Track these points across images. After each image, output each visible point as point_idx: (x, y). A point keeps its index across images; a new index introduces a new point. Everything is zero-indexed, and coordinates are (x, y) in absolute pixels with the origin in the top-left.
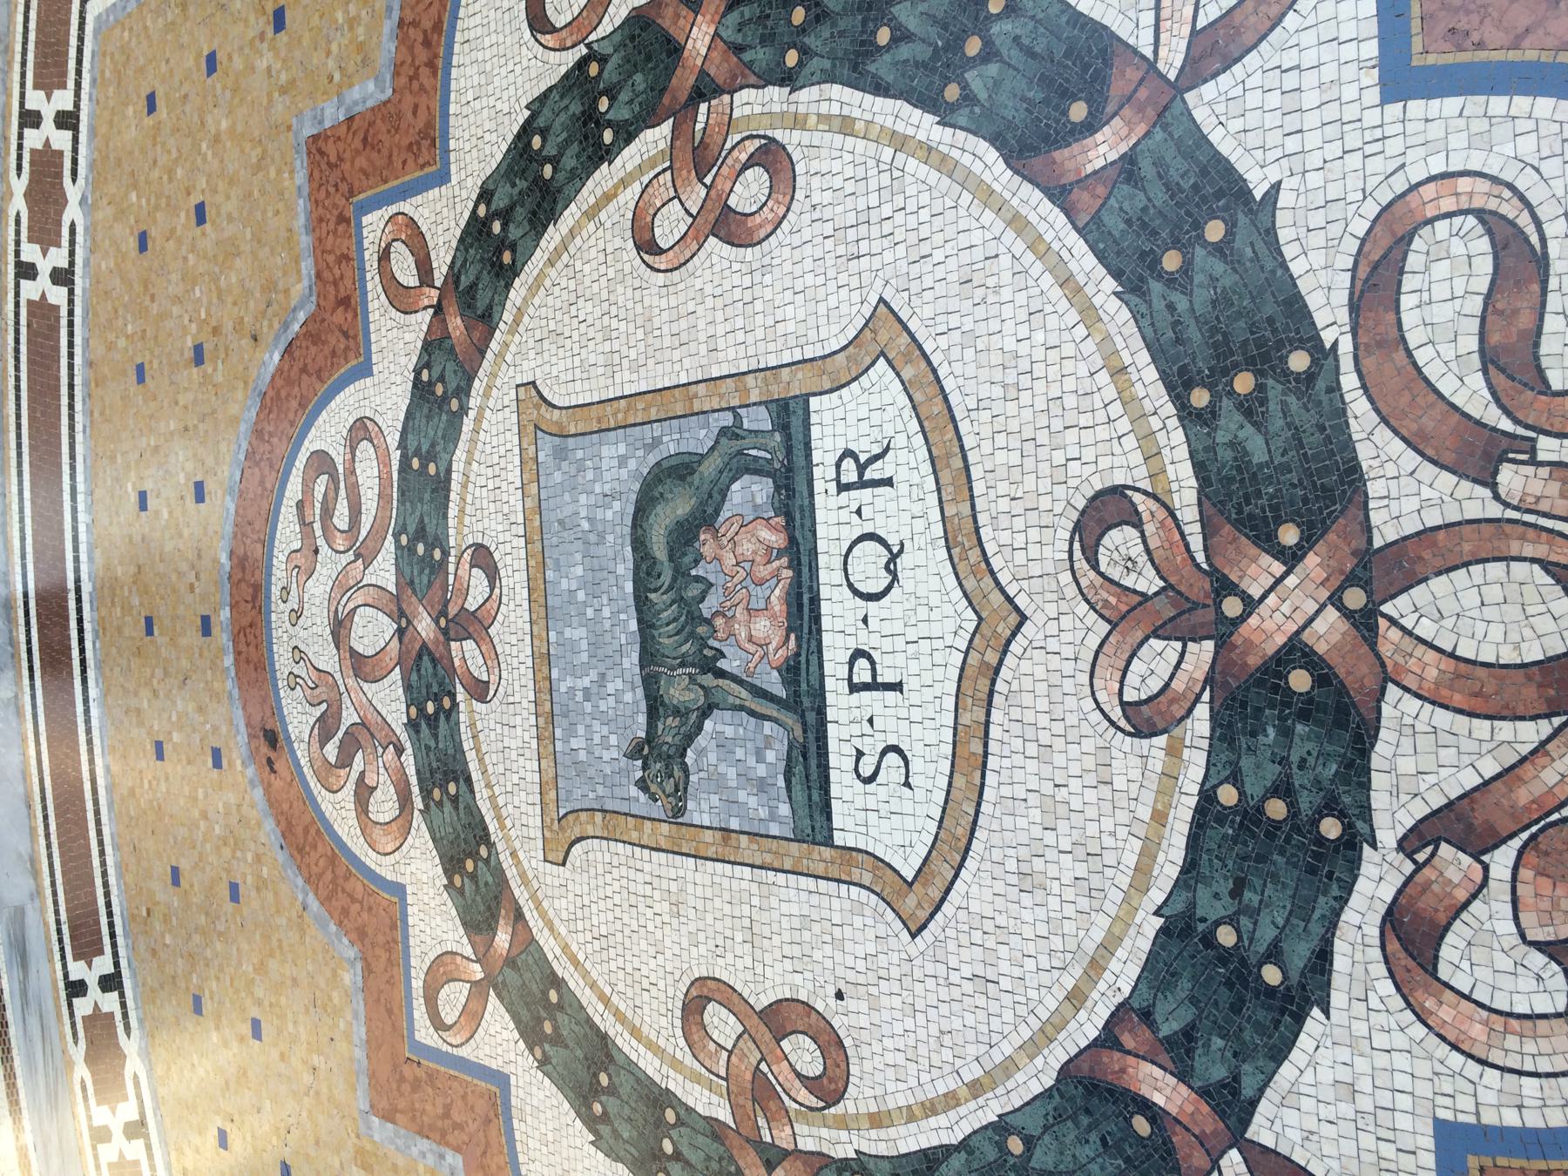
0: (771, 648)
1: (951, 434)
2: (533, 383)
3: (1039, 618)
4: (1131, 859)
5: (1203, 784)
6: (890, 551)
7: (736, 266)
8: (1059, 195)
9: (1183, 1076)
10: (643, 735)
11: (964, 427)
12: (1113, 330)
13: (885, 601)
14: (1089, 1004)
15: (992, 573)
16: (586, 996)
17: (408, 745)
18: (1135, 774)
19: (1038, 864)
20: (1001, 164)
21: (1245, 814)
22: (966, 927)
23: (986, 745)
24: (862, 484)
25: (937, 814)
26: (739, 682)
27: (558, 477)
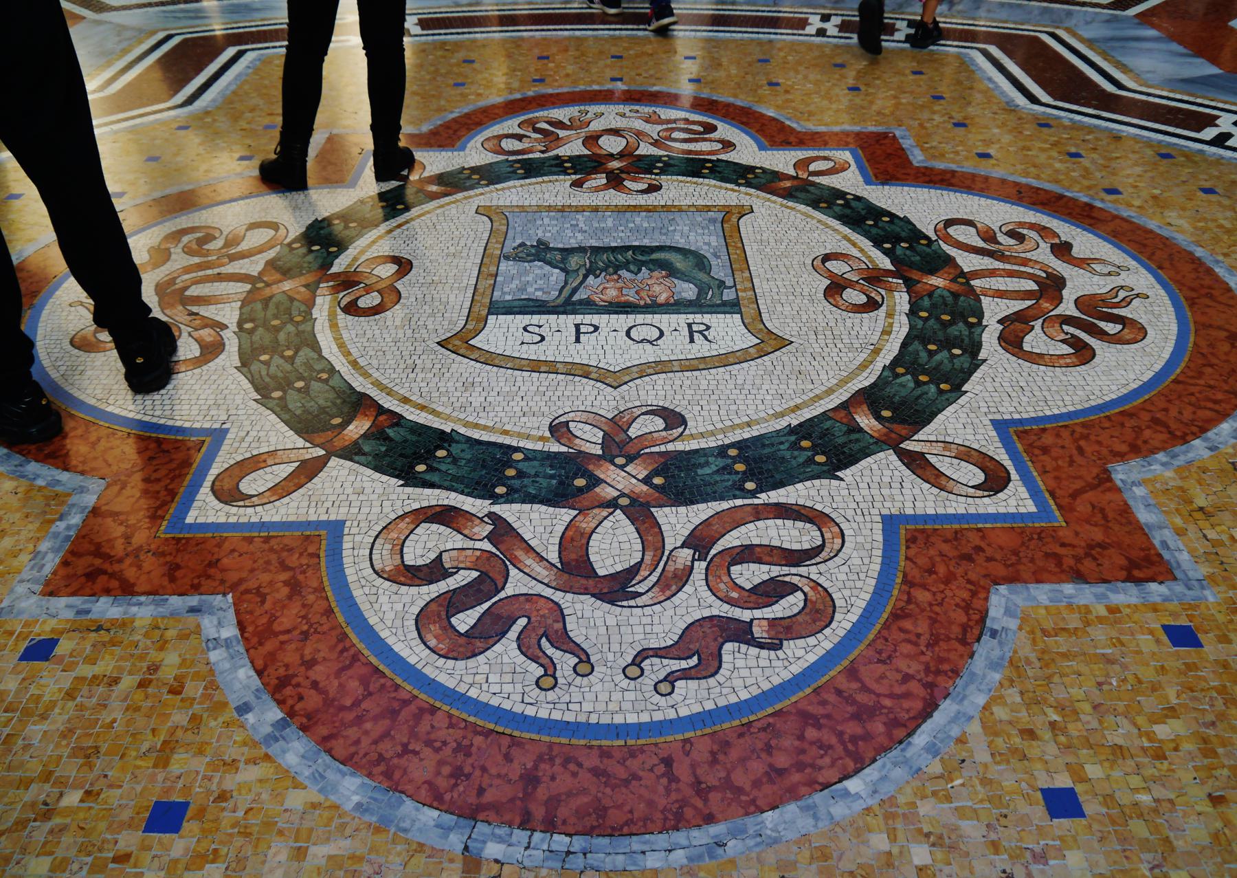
27: (699, 219)
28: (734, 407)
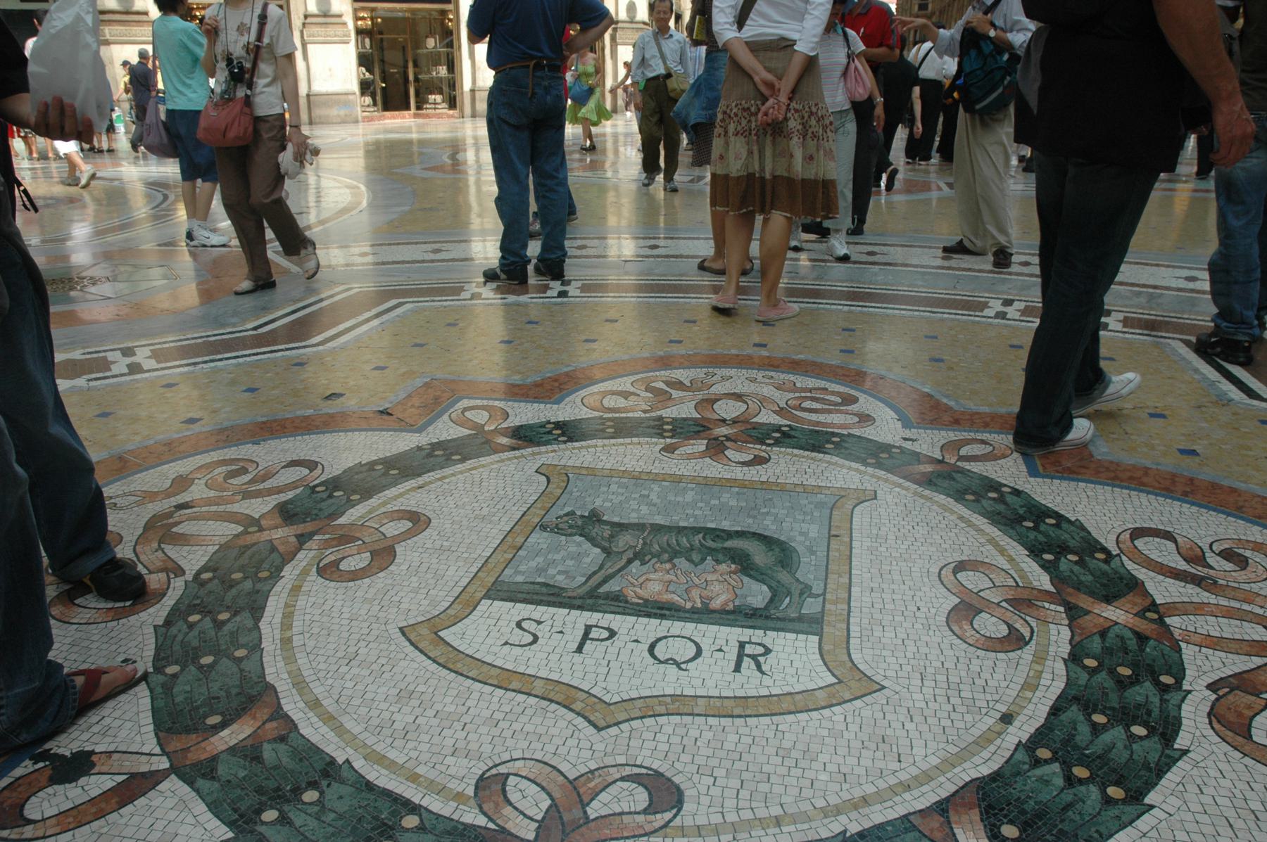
0: (638, 590)
1: (762, 711)
2: (876, 498)
4: (392, 755)
5: (426, 809)
6: (684, 663)
7: (933, 611)
8: (942, 808)
9: (232, 750)
10: (605, 518)
11: (766, 720)
12: (814, 824)
13: (647, 654)
14: (307, 710)
16: (447, 471)
17: (647, 415)
18: (452, 771)
19: (415, 703)
20: (975, 775)
21: (392, 828)
22: (392, 656)
24: (740, 656)
26: (620, 570)
28: (764, 787)
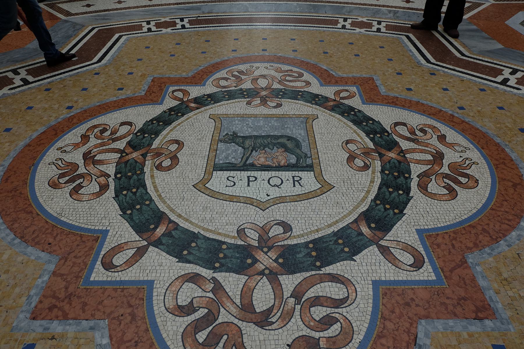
1: (304, 199)
3: (263, 213)
4: (210, 228)
9: (163, 235)
11: (306, 201)
13: (268, 184)
14: (178, 218)
15: (274, 205)
18: (229, 230)
19: (209, 210)
22: (195, 196)
23: (235, 202)
24: (294, 181)
25: (220, 192)
